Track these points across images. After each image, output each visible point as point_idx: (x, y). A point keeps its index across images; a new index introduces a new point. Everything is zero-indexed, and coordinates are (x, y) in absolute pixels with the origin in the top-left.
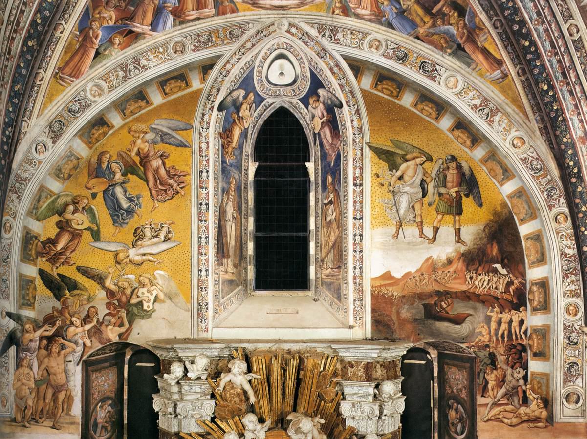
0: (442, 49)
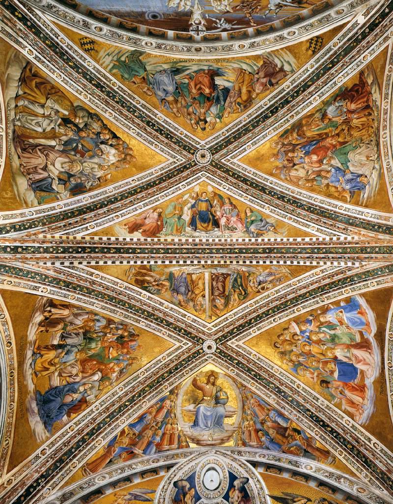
0: (297, 455)
